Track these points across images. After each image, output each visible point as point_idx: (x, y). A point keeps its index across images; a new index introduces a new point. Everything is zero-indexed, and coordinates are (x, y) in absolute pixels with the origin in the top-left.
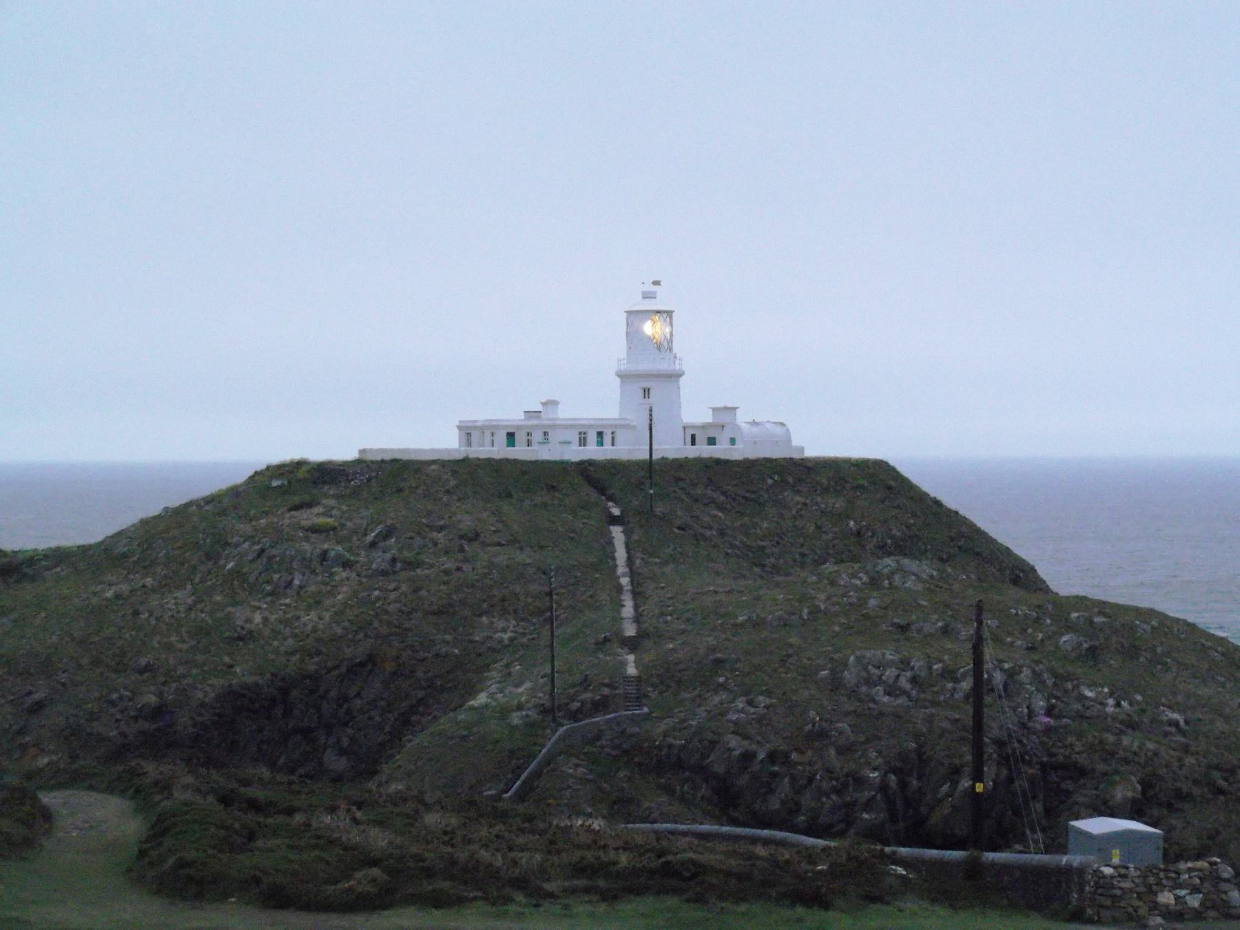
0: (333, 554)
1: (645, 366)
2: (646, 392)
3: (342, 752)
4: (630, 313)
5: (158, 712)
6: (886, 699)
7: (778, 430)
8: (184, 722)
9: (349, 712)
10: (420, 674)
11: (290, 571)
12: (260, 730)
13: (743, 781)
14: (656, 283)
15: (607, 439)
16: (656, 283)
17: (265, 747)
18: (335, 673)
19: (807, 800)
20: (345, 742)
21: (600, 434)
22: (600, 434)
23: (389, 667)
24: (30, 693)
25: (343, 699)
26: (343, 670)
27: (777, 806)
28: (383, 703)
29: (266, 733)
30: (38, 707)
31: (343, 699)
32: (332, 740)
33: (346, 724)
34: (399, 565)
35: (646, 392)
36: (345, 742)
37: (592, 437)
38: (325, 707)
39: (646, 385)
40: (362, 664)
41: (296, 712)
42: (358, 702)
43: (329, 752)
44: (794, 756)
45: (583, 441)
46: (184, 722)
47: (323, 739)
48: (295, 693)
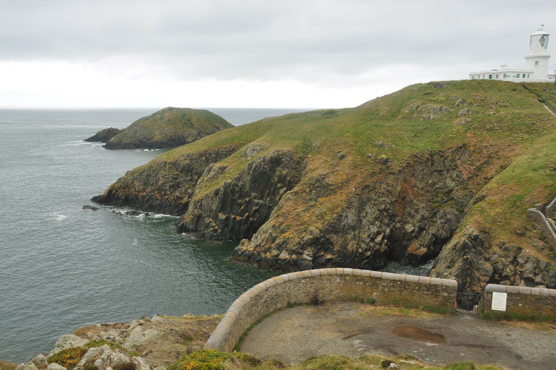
0: (444, 108)
1: (537, 54)
2: (537, 63)
5: (386, 161)
8: (396, 166)
9: (456, 165)
10: (484, 152)
11: (429, 113)
12: (423, 170)
14: (543, 25)
15: (526, 76)
16: (543, 25)
17: (424, 176)
21: (524, 75)
22: (524, 75)
23: (472, 149)
24: (340, 152)
25: (453, 161)
26: (454, 149)
29: (425, 171)
30: (343, 157)
31: (453, 161)
32: (449, 175)
33: (454, 169)
34: (470, 112)
35: (537, 63)
37: (521, 75)
38: (447, 163)
39: (537, 60)
40: (460, 147)
41: (436, 164)
42: (459, 161)
45: (518, 76)
46: (396, 166)
48: (436, 157)
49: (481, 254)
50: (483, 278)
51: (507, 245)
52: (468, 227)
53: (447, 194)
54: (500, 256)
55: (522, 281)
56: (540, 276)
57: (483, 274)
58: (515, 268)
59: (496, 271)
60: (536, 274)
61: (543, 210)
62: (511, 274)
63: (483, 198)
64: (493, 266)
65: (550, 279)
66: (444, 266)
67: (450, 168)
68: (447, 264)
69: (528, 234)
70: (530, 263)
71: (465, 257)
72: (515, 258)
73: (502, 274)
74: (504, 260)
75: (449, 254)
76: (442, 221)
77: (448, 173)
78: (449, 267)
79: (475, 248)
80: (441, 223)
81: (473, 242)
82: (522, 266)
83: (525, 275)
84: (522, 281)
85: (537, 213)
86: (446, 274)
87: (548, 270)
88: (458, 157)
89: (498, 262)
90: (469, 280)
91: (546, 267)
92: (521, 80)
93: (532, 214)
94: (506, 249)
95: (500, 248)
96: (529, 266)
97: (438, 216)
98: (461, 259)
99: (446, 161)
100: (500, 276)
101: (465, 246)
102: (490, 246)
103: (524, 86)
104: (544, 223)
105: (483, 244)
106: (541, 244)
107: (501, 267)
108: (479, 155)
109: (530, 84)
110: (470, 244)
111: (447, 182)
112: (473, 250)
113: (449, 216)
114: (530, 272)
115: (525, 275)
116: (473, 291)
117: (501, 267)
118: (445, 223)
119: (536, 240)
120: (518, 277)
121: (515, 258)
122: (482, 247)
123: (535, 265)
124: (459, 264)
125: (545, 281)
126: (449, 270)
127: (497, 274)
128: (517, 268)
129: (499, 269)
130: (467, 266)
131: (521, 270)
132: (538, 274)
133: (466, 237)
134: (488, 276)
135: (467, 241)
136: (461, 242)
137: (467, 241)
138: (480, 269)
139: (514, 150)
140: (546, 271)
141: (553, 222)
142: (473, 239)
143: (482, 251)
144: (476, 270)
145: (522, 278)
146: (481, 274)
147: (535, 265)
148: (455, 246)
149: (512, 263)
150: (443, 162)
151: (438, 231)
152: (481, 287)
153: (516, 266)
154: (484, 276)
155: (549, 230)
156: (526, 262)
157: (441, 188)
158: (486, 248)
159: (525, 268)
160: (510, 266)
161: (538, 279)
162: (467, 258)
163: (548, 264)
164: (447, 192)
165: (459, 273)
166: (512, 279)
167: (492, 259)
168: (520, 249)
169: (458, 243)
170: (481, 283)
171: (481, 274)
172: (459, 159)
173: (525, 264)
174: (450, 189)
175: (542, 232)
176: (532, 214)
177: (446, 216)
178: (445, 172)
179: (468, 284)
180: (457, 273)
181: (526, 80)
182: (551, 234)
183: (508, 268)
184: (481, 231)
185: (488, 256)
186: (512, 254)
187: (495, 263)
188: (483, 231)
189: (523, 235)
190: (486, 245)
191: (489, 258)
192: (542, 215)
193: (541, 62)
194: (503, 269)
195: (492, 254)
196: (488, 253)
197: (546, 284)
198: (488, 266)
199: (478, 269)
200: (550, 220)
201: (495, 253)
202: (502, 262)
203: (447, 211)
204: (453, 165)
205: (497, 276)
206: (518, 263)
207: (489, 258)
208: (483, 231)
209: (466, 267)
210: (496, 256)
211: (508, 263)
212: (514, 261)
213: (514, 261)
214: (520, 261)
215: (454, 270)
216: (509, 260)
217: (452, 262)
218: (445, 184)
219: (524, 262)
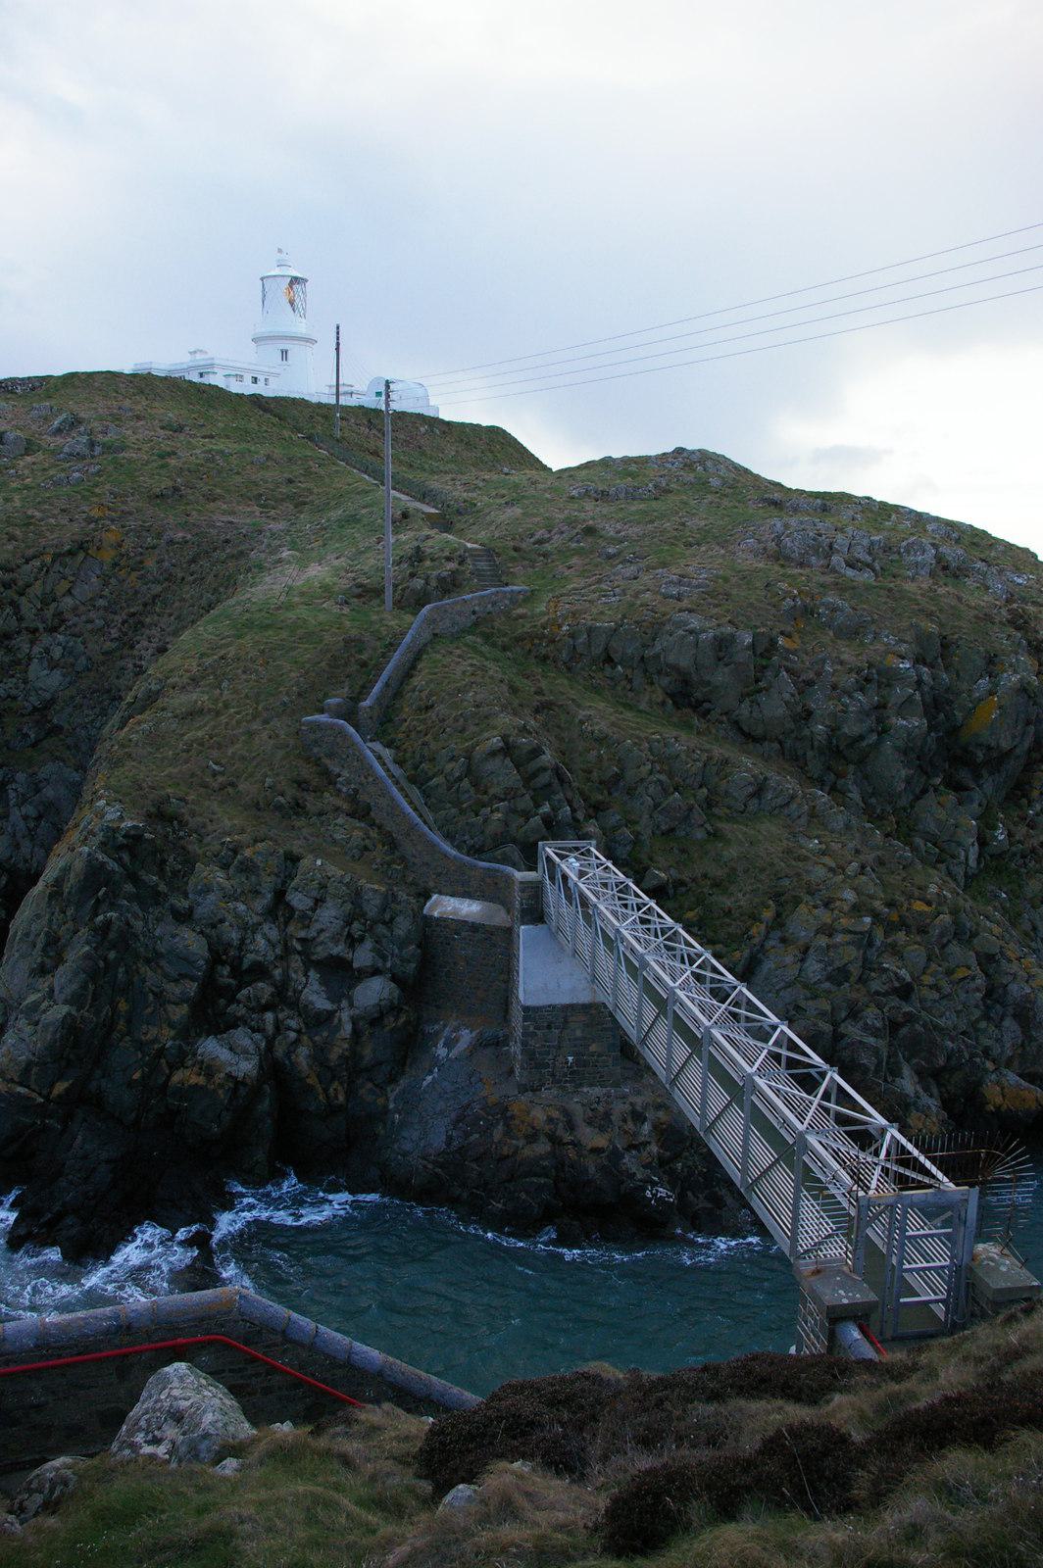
2: (284, 354)
3: (53, 665)
4: (262, 279)
6: (850, 573)
7: (420, 392)
9: (59, 614)
10: (150, 563)
13: (721, 676)
15: (261, 383)
18: (37, 563)
19: (821, 703)
20: (57, 653)
23: (108, 556)
27: (781, 711)
28: (101, 602)
31: (49, 599)
32: (36, 649)
34: (98, 450)
35: (284, 354)
36: (57, 653)
37: (248, 379)
40: (71, 553)
42: (69, 600)
43: (35, 664)
44: (781, 641)
47: (26, 647)
49: (157, 897)
50: (174, 990)
51: (248, 853)
52: (102, 802)
53: (37, 716)
54: (230, 897)
55: (312, 973)
56: (368, 944)
57: (174, 974)
58: (283, 931)
59: (217, 956)
60: (353, 942)
61: (350, 714)
62: (271, 957)
63: (151, 698)
64: (207, 936)
65: (401, 949)
66: (24, 966)
67: (41, 626)
68: (37, 956)
69: (312, 803)
70: (330, 903)
71: (101, 918)
72: (280, 895)
73: (240, 958)
74: (242, 907)
75: (38, 916)
76: (29, 810)
77: (32, 643)
78: (42, 971)
79: (133, 877)
80: (25, 818)
81: (126, 857)
82: (306, 920)
83: (320, 952)
84: (312, 973)
85: (332, 726)
86: (32, 998)
87: (392, 919)
88: (64, 585)
89: (222, 921)
90: (123, 1006)
91: (384, 908)
92: (246, 388)
93: (319, 735)
94: (248, 868)
95: (225, 867)
96: (329, 915)
97: (12, 794)
98: (84, 932)
99: (23, 600)
100: (236, 972)
101: (95, 875)
102: (189, 862)
103: (257, 400)
104: (361, 759)
105: (164, 861)
106: (357, 832)
107: (235, 936)
108: (135, 574)
109: (277, 400)
110: (112, 865)
111: (31, 675)
112: (129, 888)
113: (49, 792)
114: (335, 939)
115: (319, 949)
116: (141, 1046)
117: (235, 936)
118: (39, 817)
119: (340, 821)
120: (296, 962)
121: (280, 895)
122: (161, 873)
123: (348, 906)
124: (79, 950)
125: (384, 958)
126: (43, 984)
127: (223, 963)
128: (291, 929)
129: (229, 945)
130: (112, 955)
131: (302, 934)
132: (362, 939)
133: (95, 841)
134: (193, 979)
135: (100, 857)
136: (79, 865)
137: (100, 857)
138: (159, 955)
139: (241, 553)
140: (385, 923)
141: (387, 753)
142: (121, 847)
143: (162, 888)
144: (148, 961)
145: (309, 963)
146: (166, 975)
147: (348, 906)
148: (58, 883)
149: (271, 913)
150: (12, 603)
151: (17, 846)
152: (171, 1025)
153: (286, 924)
154: (176, 981)
155: (377, 779)
156: (319, 902)
157: (15, 698)
158: (175, 873)
159: (318, 926)
160: (266, 927)
161: (363, 957)
162: (108, 923)
163: (389, 899)
164: (35, 709)
165: (84, 987)
166: (277, 973)
167: (199, 911)
168: (293, 859)
169: (66, 870)
170: (170, 1008)
171: (166, 975)
172: (69, 592)
173: (314, 910)
174: (48, 696)
175: (356, 791)
176: (319, 735)
177: (38, 791)
178: (22, 642)
179: (121, 1025)
180: (75, 986)
181: (259, 389)
182: (384, 793)
183: (259, 937)
184: (149, 815)
185: (186, 904)
186: (268, 883)
187: (214, 926)
188: (160, 815)
189: (298, 808)
190: (173, 862)
191: (191, 909)
192: (352, 730)
193: (295, 350)
194: (242, 940)
195: (199, 893)
196: (186, 896)
197: (390, 970)
198: (192, 942)
199: (154, 959)
200: (378, 746)
201: (207, 890)
202: (237, 916)
203: (41, 776)
204: (49, 613)
205: (226, 970)
206: (292, 909)
207: (191, 909)
208: (160, 815)
209: (105, 959)
210: (212, 897)
211: (256, 919)
212: (279, 908)
213: (279, 908)
214: (298, 900)
215: (63, 978)
216: (260, 904)
217: (54, 947)
218: (25, 682)
219: (310, 903)
